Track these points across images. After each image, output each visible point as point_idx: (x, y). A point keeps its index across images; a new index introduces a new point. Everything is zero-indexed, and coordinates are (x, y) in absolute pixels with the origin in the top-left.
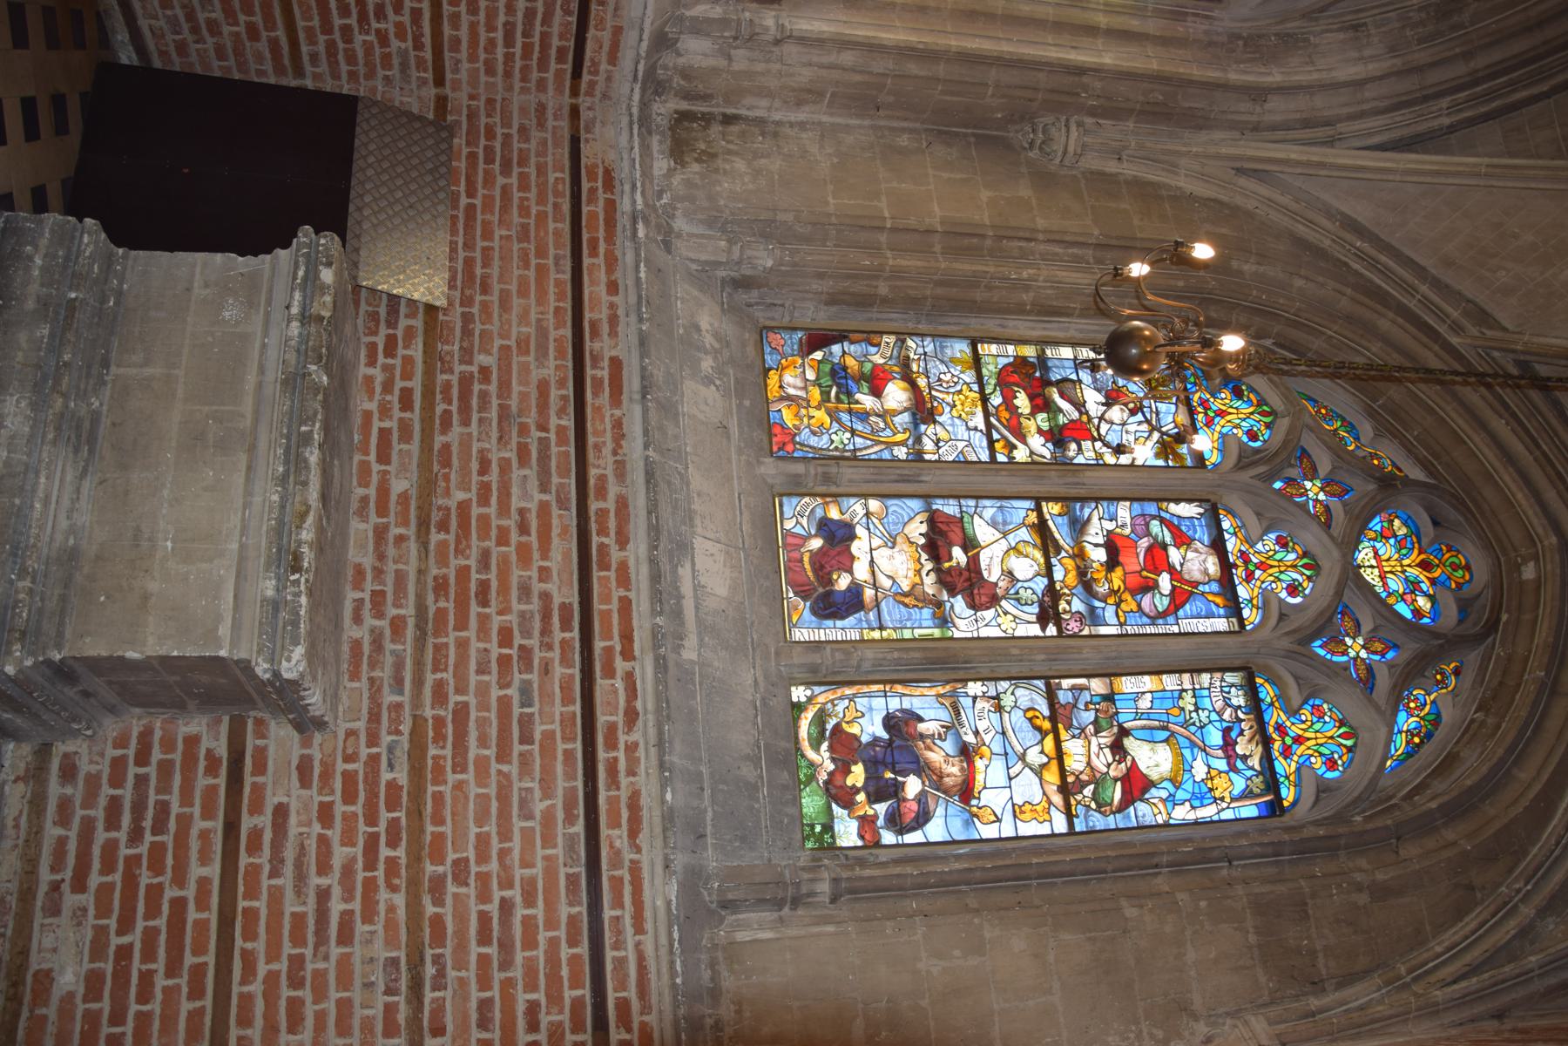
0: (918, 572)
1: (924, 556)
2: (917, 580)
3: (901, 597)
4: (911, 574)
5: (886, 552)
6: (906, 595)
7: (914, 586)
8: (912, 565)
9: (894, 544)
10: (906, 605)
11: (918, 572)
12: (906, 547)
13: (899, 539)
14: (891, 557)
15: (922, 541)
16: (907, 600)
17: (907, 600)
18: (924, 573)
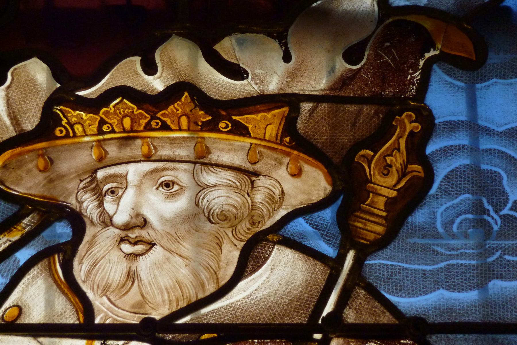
0: (221, 114)
1: (127, 72)
2: (267, 124)
3: (355, 222)
4: (229, 150)
5: (100, 263)
6: (349, 189)
7: (296, 142)
8: (176, 142)
9: (52, 210)
10: (414, 194)
11: (221, 114)
12: (75, 160)
13: (28, 184)
14: (135, 233)
15: (37, 73)
16: (385, 187)
17: (385, 187)
18: (217, 83)
